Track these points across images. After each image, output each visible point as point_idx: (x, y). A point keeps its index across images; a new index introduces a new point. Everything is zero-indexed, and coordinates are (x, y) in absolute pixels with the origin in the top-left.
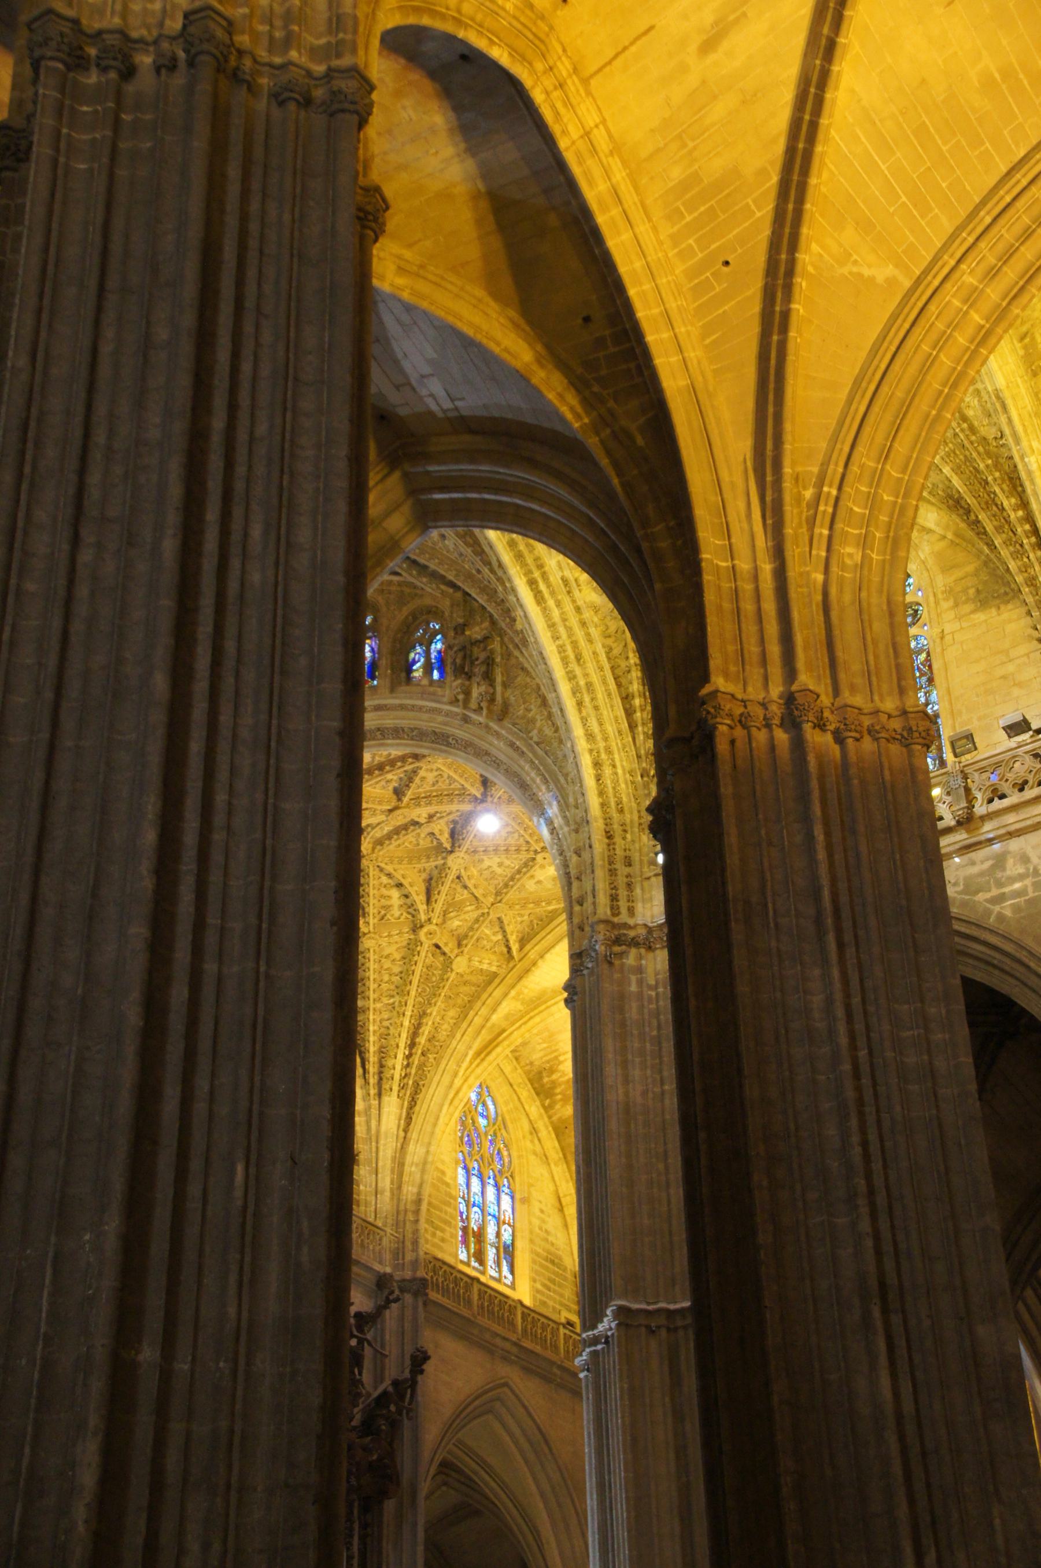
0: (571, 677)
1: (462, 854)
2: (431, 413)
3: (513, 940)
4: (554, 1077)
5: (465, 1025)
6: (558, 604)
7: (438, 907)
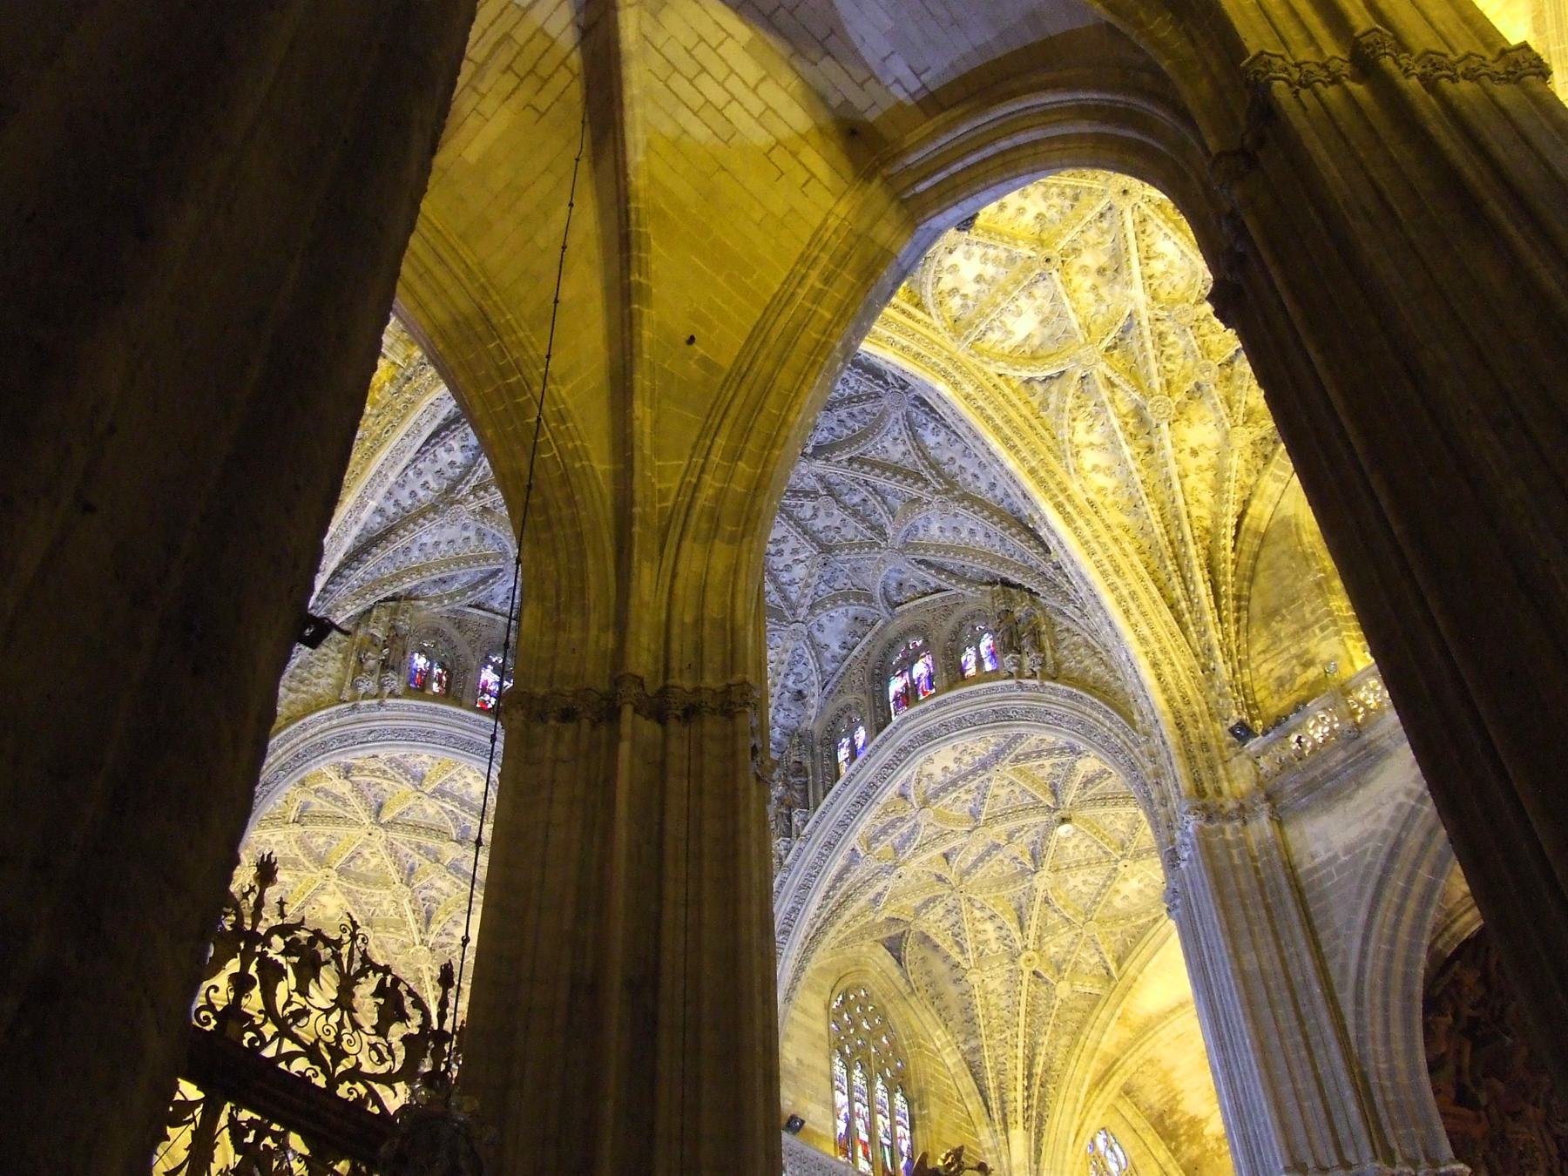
0: (1113, 588)
1: (1046, 873)
2: (900, 105)
3: (1109, 958)
4: (1175, 1118)
5: (1077, 1051)
6: (1088, 523)
7: (1032, 933)
